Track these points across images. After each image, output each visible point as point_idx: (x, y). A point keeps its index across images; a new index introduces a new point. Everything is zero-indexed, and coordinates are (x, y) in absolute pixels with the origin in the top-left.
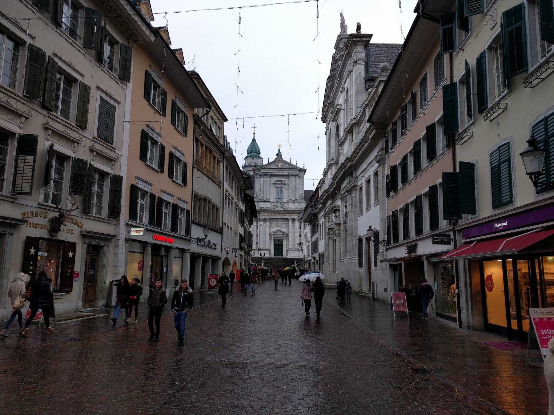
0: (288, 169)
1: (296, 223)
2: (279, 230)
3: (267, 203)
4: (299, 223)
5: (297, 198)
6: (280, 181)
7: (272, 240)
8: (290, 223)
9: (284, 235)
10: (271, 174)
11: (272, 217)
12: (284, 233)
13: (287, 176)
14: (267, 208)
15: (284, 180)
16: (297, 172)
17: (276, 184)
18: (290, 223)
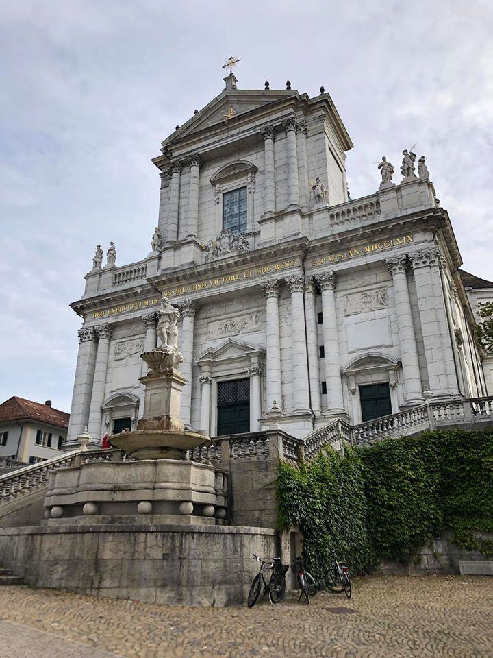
0: (253, 112)
1: (297, 297)
2: (231, 344)
3: (183, 249)
4: (310, 297)
5: (294, 199)
6: (234, 167)
7: (206, 387)
8: (272, 303)
9: (248, 358)
10: (200, 151)
11: (200, 296)
12: (245, 348)
13: (256, 142)
14: (182, 265)
15: (252, 159)
16: (291, 110)
17: (221, 181)
18: (272, 303)
